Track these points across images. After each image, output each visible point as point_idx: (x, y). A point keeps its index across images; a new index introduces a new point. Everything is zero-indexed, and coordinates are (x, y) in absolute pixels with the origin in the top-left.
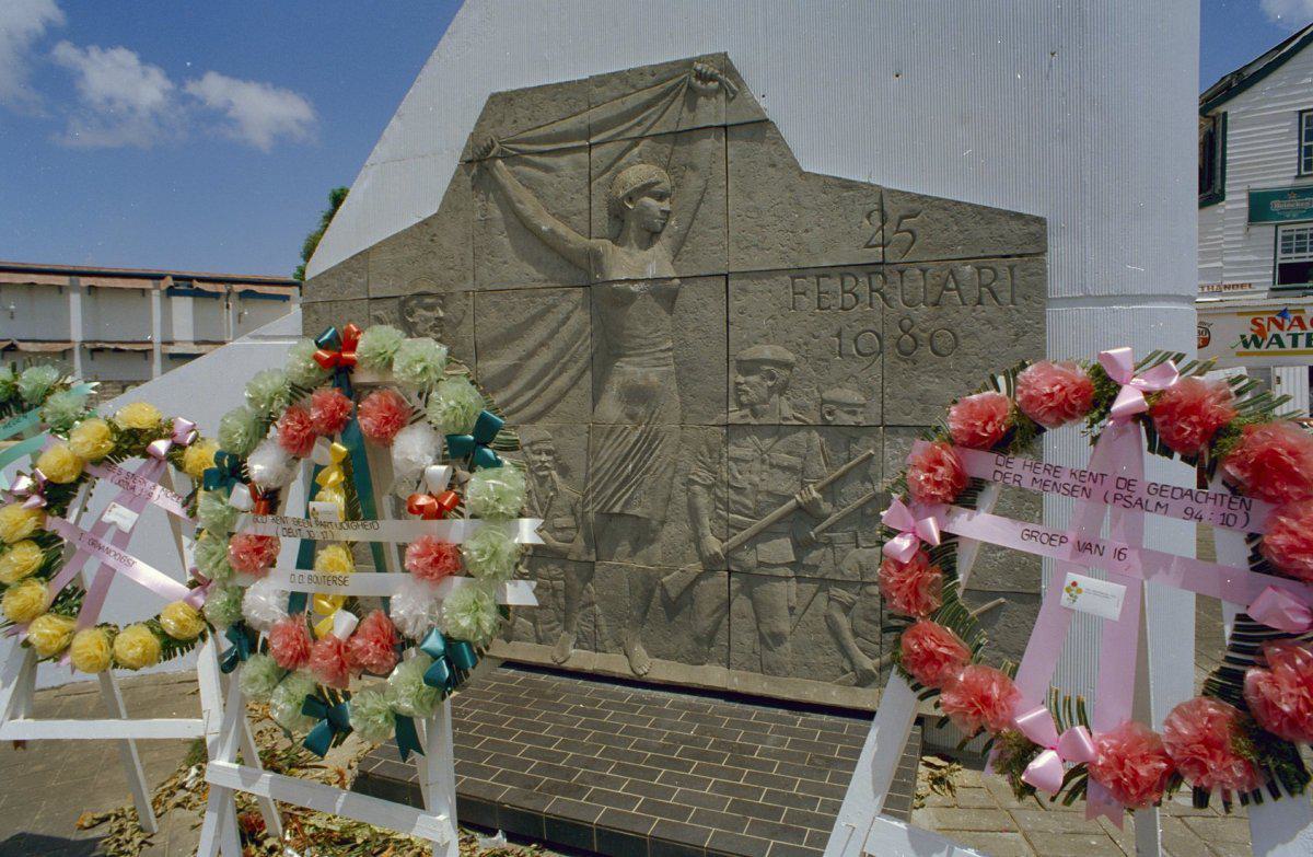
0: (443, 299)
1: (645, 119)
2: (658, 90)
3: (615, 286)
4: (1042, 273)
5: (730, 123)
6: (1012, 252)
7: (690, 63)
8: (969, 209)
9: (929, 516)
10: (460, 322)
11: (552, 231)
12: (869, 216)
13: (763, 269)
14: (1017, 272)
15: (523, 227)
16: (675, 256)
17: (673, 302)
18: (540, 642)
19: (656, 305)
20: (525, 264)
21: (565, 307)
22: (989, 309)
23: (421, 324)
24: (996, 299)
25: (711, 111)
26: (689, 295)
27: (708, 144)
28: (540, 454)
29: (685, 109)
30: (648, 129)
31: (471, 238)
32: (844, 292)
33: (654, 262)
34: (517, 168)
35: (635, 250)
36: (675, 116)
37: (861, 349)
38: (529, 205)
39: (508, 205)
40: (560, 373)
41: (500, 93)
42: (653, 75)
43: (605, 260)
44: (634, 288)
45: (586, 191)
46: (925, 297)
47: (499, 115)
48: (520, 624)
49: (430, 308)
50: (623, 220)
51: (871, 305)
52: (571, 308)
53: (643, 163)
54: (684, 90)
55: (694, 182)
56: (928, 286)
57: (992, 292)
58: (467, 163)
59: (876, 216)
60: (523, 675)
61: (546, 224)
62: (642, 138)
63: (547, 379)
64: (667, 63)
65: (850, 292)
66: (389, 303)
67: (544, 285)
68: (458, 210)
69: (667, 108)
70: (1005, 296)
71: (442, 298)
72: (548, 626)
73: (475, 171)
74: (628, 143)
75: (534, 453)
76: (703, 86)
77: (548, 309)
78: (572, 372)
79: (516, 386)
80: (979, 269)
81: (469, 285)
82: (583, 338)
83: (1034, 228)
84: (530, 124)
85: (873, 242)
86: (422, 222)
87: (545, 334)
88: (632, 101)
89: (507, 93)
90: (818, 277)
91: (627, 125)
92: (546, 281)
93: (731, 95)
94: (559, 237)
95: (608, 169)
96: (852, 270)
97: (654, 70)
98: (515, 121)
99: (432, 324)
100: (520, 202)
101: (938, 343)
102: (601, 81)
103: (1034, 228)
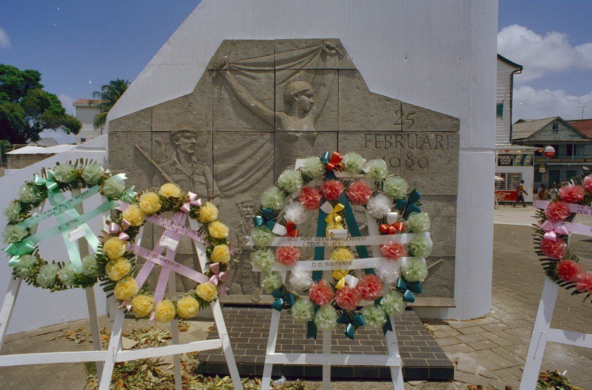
0: (196, 134)
1: (303, 62)
2: (308, 50)
3: (289, 133)
4: (458, 139)
5: (341, 68)
6: (447, 130)
7: (323, 41)
8: (433, 113)
9: (358, 230)
10: (205, 146)
11: (256, 106)
12: (396, 113)
13: (353, 130)
14: (450, 138)
15: (240, 103)
16: (315, 122)
17: (314, 142)
18: (244, 293)
19: (307, 143)
20: (241, 120)
21: (262, 141)
22: (439, 151)
23: (183, 145)
24: (442, 147)
25: (332, 62)
26: (320, 139)
27: (330, 76)
28: (247, 207)
29: (320, 60)
30: (303, 66)
31: (211, 106)
32: (386, 141)
33: (306, 124)
34: (237, 76)
35: (297, 118)
36: (316, 62)
37: (392, 164)
38: (244, 94)
39: (233, 93)
40: (258, 171)
41: (229, 40)
42: (306, 43)
43: (283, 122)
44: (298, 135)
45: (273, 90)
46: (417, 146)
47: (228, 50)
48: (234, 286)
49: (189, 138)
50: (290, 103)
51: (396, 147)
52: (264, 142)
53: (301, 80)
54: (320, 52)
55: (324, 91)
56: (418, 141)
57: (441, 145)
58: (210, 71)
59: (399, 112)
60: (239, 310)
61: (253, 103)
62: (300, 70)
63: (251, 173)
64: (312, 39)
65: (388, 142)
66: (163, 134)
67: (251, 131)
68: (204, 92)
69: (312, 59)
70: (445, 146)
71: (195, 134)
72: (249, 286)
73: (214, 74)
74: (294, 71)
75: (243, 207)
76: (329, 52)
77: (252, 142)
78: (264, 170)
79: (236, 175)
80: (436, 136)
81: (210, 129)
82: (270, 155)
83: (456, 122)
84: (245, 57)
85: (398, 123)
86: (184, 96)
87: (250, 153)
88: (296, 53)
89: (232, 41)
90: (376, 135)
91: (294, 63)
92: (251, 129)
93: (341, 57)
94: (260, 109)
95: (284, 81)
96: (388, 133)
97: (306, 41)
98: (237, 54)
99: (189, 146)
100: (240, 92)
101: (421, 163)
102: (282, 42)
103: (456, 122)
